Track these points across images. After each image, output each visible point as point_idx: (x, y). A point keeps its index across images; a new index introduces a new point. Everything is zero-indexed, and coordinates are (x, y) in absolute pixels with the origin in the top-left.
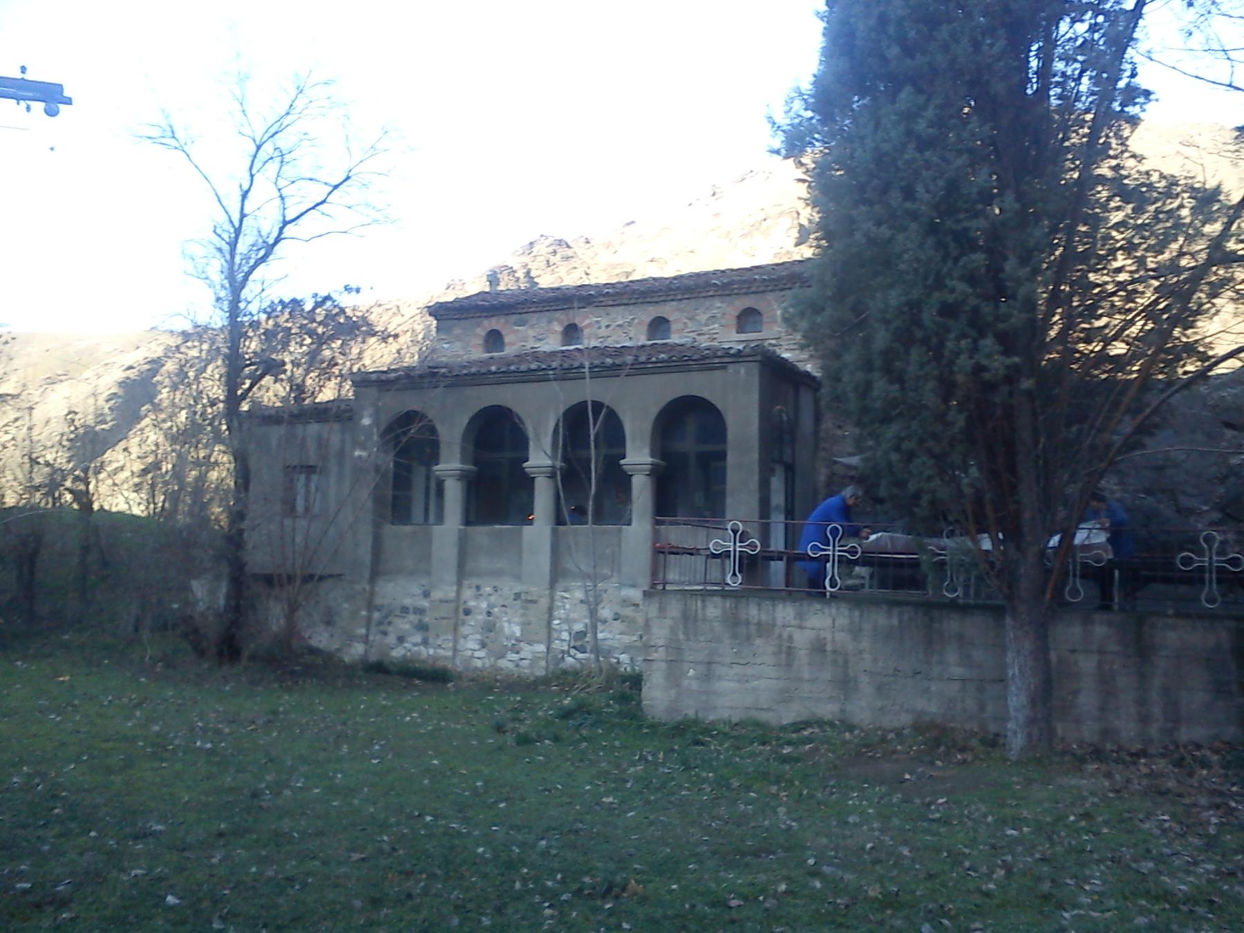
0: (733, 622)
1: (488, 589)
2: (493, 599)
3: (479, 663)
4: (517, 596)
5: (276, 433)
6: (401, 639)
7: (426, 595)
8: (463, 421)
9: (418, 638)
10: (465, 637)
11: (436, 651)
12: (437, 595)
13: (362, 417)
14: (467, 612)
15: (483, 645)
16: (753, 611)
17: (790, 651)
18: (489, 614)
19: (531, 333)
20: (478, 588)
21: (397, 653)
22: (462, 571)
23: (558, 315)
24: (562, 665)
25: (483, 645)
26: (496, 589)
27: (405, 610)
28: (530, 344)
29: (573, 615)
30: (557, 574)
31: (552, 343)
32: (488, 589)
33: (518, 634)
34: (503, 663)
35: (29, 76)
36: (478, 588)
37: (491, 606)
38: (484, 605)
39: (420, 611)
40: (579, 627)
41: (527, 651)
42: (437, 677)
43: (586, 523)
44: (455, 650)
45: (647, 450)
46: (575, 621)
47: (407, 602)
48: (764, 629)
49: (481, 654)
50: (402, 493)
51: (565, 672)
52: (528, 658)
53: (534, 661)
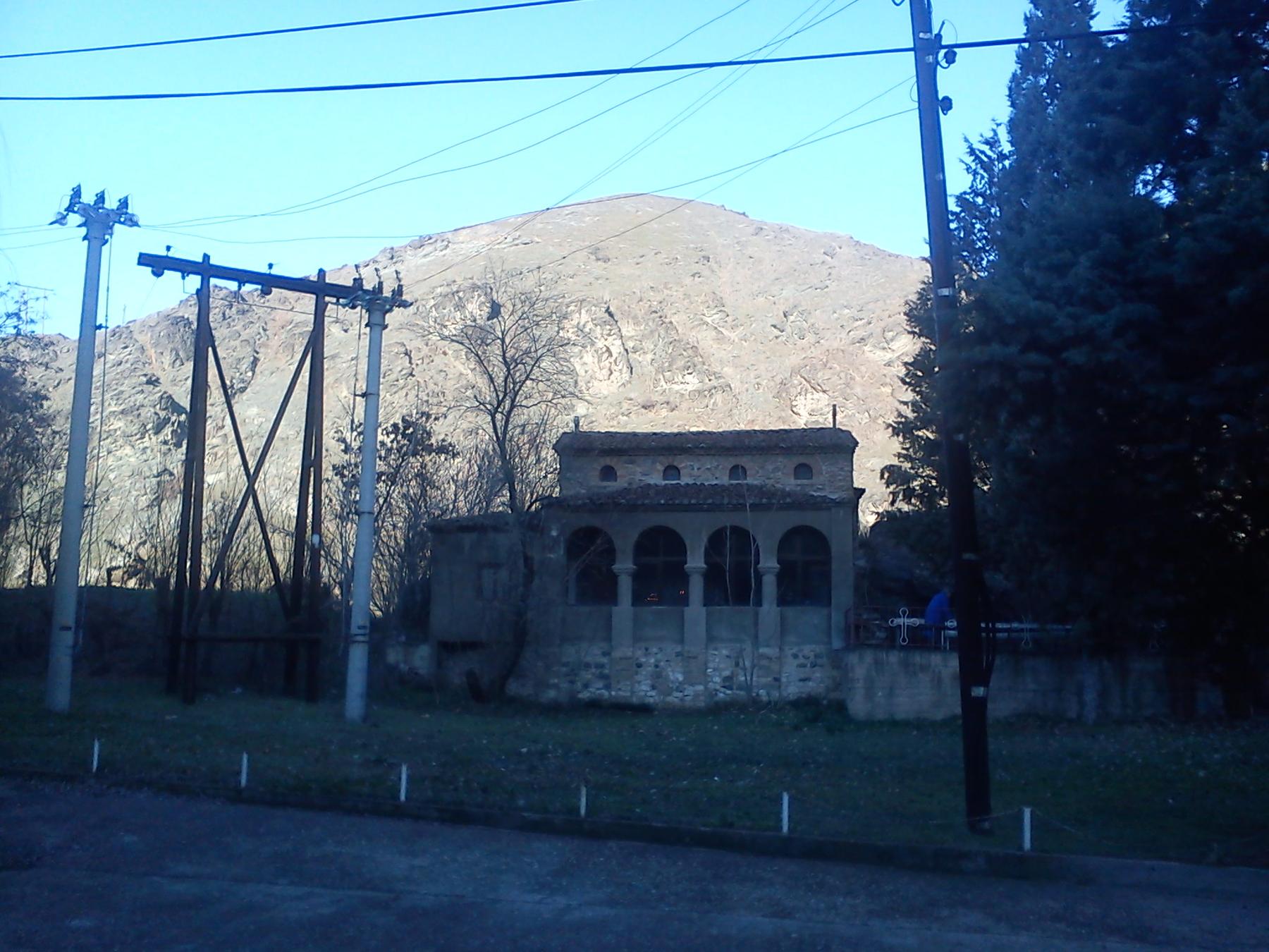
0: (906, 665)
1: (655, 650)
2: (659, 656)
3: (651, 700)
4: (678, 654)
5: (468, 539)
6: (586, 686)
7: (605, 654)
8: (634, 536)
9: (600, 684)
10: (639, 682)
11: (621, 692)
12: (617, 654)
13: (551, 530)
14: (639, 666)
15: (653, 687)
16: (917, 658)
17: (940, 680)
18: (657, 666)
19: (639, 469)
20: (647, 649)
21: (585, 695)
22: (637, 639)
23: (661, 458)
24: (716, 699)
25: (653, 687)
26: (661, 649)
27: (588, 666)
28: (639, 477)
29: (722, 666)
30: (711, 639)
31: (656, 479)
32: (655, 650)
33: (681, 679)
34: (669, 699)
35: (274, 272)
36: (647, 649)
37: (658, 661)
38: (652, 660)
39: (602, 666)
40: (727, 673)
41: (690, 690)
42: (644, 709)
43: (748, 604)
44: (633, 692)
45: (775, 560)
46: (724, 670)
47: (589, 659)
48: (923, 668)
49: (653, 693)
50: (598, 587)
51: (717, 703)
52: (693, 694)
53: (696, 695)
